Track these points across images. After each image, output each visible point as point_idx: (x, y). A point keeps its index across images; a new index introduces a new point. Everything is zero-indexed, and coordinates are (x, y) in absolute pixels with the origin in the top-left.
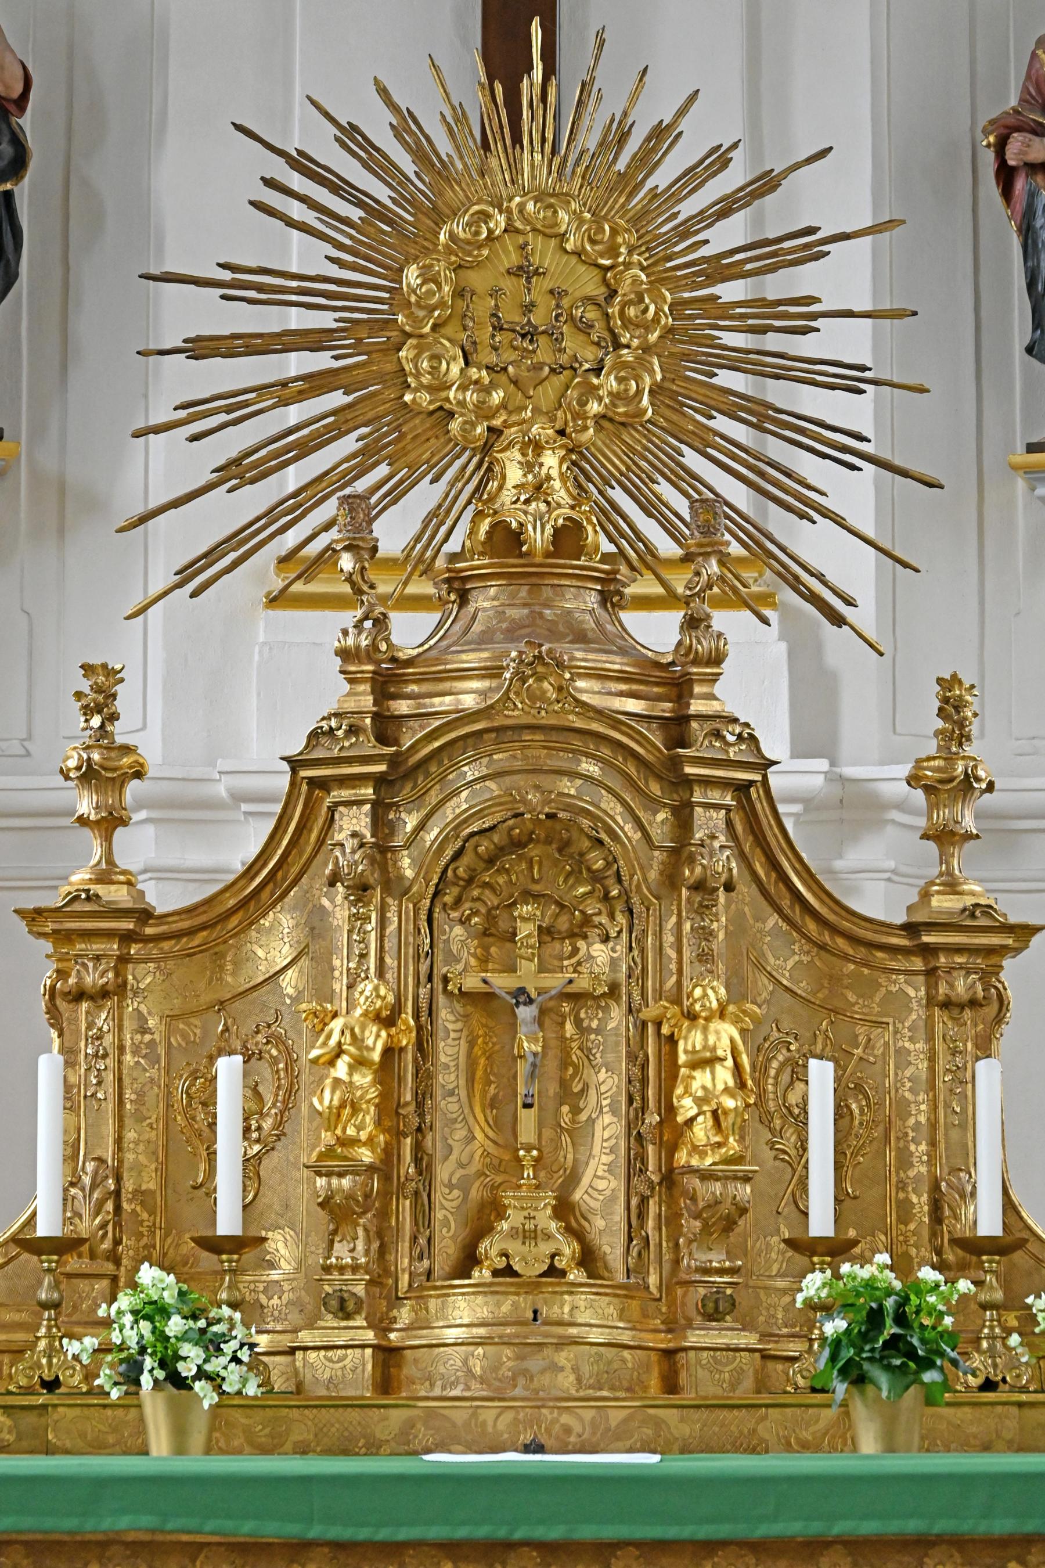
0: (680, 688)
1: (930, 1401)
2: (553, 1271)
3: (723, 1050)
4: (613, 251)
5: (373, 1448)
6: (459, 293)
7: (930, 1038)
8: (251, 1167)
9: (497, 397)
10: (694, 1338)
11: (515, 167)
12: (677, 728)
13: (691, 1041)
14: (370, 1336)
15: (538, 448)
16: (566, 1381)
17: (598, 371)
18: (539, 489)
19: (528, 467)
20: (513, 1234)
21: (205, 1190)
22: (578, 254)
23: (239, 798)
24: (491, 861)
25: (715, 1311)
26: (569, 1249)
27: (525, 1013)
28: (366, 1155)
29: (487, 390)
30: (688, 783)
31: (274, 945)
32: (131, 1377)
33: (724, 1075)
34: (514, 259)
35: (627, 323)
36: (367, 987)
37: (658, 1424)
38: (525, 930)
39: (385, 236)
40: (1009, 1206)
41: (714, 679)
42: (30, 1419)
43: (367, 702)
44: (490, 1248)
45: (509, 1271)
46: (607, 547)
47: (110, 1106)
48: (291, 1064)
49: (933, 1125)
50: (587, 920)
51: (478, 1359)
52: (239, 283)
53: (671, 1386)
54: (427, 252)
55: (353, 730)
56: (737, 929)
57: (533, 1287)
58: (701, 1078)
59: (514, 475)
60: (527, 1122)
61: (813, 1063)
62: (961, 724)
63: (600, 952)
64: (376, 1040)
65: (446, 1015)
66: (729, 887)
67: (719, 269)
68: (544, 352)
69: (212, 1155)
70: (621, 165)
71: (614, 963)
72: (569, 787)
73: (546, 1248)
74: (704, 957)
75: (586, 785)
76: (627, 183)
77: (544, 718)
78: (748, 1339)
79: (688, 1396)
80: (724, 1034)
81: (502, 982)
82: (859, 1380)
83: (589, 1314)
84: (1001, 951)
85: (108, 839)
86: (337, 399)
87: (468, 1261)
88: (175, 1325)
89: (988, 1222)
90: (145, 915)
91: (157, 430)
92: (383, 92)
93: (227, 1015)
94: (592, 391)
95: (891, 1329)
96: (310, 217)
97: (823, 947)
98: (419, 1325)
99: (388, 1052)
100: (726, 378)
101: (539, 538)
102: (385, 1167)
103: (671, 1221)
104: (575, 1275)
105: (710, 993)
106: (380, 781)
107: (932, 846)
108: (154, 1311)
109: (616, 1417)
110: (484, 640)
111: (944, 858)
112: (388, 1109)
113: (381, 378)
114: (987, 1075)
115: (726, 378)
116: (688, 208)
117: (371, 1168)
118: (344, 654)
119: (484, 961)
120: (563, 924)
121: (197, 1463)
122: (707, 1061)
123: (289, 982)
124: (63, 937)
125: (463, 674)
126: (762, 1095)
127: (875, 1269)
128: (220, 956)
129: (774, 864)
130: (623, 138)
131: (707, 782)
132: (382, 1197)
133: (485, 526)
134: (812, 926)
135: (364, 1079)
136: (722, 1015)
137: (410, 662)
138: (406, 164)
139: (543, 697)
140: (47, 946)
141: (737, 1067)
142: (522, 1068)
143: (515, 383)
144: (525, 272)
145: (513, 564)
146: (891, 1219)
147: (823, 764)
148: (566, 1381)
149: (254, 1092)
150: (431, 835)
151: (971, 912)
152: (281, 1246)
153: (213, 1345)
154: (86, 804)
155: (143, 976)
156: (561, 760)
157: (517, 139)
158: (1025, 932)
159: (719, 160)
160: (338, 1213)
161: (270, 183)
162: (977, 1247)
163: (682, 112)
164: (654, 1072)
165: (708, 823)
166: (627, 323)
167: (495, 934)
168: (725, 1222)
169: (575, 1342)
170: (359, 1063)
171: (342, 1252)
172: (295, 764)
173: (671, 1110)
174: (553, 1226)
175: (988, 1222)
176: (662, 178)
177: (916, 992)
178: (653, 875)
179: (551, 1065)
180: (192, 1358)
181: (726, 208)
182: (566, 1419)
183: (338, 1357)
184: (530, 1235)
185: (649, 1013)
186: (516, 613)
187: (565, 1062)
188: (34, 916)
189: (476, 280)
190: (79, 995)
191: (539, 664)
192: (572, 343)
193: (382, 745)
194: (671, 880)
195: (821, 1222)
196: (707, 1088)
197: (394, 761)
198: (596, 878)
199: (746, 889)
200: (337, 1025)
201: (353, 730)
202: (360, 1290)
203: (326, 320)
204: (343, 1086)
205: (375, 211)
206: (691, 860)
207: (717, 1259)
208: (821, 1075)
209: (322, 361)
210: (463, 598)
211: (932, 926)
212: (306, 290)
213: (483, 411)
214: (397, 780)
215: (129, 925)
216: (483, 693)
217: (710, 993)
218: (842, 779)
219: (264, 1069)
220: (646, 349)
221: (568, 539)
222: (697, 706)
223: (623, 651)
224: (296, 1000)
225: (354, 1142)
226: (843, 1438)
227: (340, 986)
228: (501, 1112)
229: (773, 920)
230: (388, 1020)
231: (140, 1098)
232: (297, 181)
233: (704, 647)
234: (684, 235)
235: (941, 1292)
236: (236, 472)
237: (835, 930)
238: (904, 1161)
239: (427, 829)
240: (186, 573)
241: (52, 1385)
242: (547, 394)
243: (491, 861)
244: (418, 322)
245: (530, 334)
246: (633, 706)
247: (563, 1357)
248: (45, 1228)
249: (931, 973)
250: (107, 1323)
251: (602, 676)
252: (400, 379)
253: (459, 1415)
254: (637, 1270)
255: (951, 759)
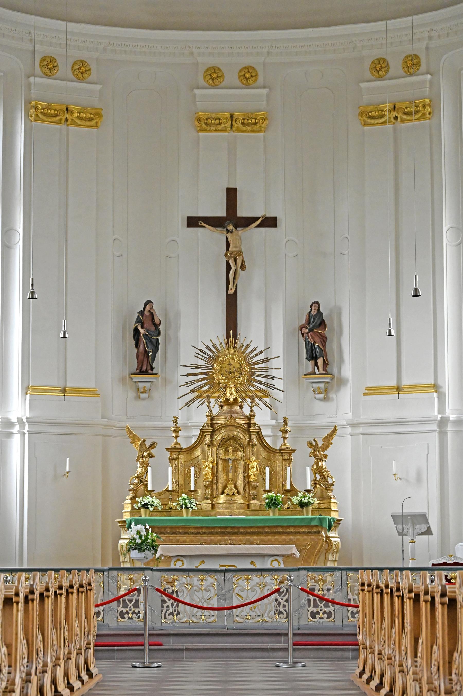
0: (250, 419)
1: (279, 510)
2: (234, 494)
3: (255, 466)
4: (241, 362)
5: (211, 516)
6: (222, 367)
7: (282, 464)
8: (196, 481)
9: (226, 381)
10: (251, 502)
11: (228, 350)
12: (249, 425)
13: (251, 465)
14: (210, 502)
15: (231, 388)
16: (235, 508)
17: (239, 377)
18: (231, 394)
19: (230, 390)
20: (229, 489)
21: (190, 484)
22: (237, 362)
23: (192, 426)
24: (225, 442)
25: (254, 499)
26: (236, 491)
27: (230, 461)
28: (210, 480)
29: (225, 380)
30: (251, 432)
31: (198, 452)
32: (181, 507)
33: (255, 469)
34: (228, 363)
35: (243, 371)
36: (210, 458)
37: (246, 513)
38: (230, 451)
39: (212, 360)
40: (291, 485)
41: (254, 418)
42: (169, 513)
43: (210, 422)
44: (226, 491)
45: (228, 494)
46: (240, 400)
47: (177, 474)
48: (200, 468)
49: (283, 475)
50: (238, 449)
51: (224, 505)
52: (193, 366)
53: (248, 508)
54: (217, 362)
55: (208, 426)
56: (257, 450)
57: (231, 496)
58: (252, 470)
59: (229, 391)
60: (230, 475)
61: (266, 468)
62: (286, 423)
63: (240, 453)
64: (211, 465)
65: (220, 462)
66: (256, 445)
67: (255, 363)
68: (232, 375)
69: (190, 479)
70: (242, 350)
71: (241, 455)
72: (235, 433)
73: (233, 491)
74: (253, 454)
75: (238, 433)
76: (243, 352)
77: (232, 424)
78: (258, 502)
79: (250, 509)
80: (255, 464)
81: (227, 457)
82: (270, 508)
83: (238, 499)
84: (291, 453)
85: (176, 439)
86: (206, 381)
87: (223, 493)
88: (187, 501)
89: (288, 487)
90: (182, 449)
91: (182, 386)
92: (211, 341)
93: (193, 462)
94: (238, 380)
95: (274, 501)
96: (202, 357)
97: (269, 452)
98: (217, 501)
99: (213, 466)
100: (256, 378)
101: (232, 400)
102: (213, 480)
103: (249, 488)
104: (237, 494)
105: (253, 458)
106: (211, 432)
107: (283, 439)
108: (184, 499)
109: (241, 512)
110: (225, 413)
111: (284, 441)
112: (213, 474)
113: (211, 379)
114: (288, 469)
115: (256, 378)
116: (251, 355)
117: (210, 481)
118: (207, 416)
119: (225, 454)
120: (235, 449)
121: (190, 517)
122: (253, 467)
123: (200, 457)
124: (170, 452)
125: (222, 418)
126: (260, 472)
127: (273, 494)
128: (191, 454)
129: (262, 442)
130: (242, 346)
131: (253, 432)
132: (213, 484)
133: (225, 398)
134: (267, 449)
135: (210, 470)
136: (255, 461)
137: (215, 416)
138: (214, 350)
139: (232, 422)
140: (169, 453)
141: (257, 468)
142: (230, 468)
143: (229, 379)
144: (230, 364)
145: (228, 404)
146: (277, 487)
147: (275, 421)
148: (235, 508)
149: (196, 471)
150: (218, 439)
151: (287, 448)
152: (199, 491)
153: (192, 503)
154: (174, 434)
155: (181, 456)
156: (235, 429)
157: (229, 347)
158: (294, 451)
159: (255, 349)
160: (206, 487)
161: (196, 353)
162: (287, 491)
163: (250, 343)
164: (247, 468)
165: (254, 437)
166: (243, 371)
167: (226, 451)
168: (255, 488)
169: (236, 503)
170: (209, 468)
171: (207, 492)
172: (201, 430)
173: (248, 474)
174: (234, 488)
175: (288, 487)
176: (248, 351)
177: (280, 458)
178: (246, 443)
179: (234, 467)
180: (189, 505)
181: (256, 355)
182: (235, 512)
183: (207, 505)
184: (230, 489)
185: (246, 461)
186: (229, 410)
187: (235, 467)
188: (167, 449)
189: (224, 366)
190: (173, 459)
191: (231, 418)
192: (236, 374)
193: (212, 426)
194: (249, 444)
195: (267, 488)
196: (253, 471)
197: (213, 430)
198: (239, 444)
199: (259, 445)
200: (206, 463)
201: (208, 426)
202: (209, 497)
203: (204, 371)
204: (207, 471)
205: (210, 357)
206: (251, 442)
207: (254, 492)
208: (267, 469)
209: (204, 376)
210: (222, 408)
211: (282, 450)
212: (201, 367)
213: (224, 383)
214: (213, 433)
215: (179, 450)
216: (225, 421)
217: (253, 458)
218: (278, 422)
219: (197, 468)
220: (246, 374)
221: (235, 400)
222: (252, 422)
223: (242, 415)
224: (201, 460)
225: (208, 478)
226: (269, 515)
227: (206, 458)
228: (227, 473)
229: (262, 449)
230: (213, 462)
231: (181, 472)
232: (199, 352)
233: (253, 414)
234: (251, 359)
235: (281, 496)
236: (192, 391)
237: (270, 450)
238: (279, 479)
239: (218, 438)
240: (186, 404)
241: (171, 509)
242: (233, 380)
243: (225, 442)
244: (216, 371)
245: (230, 373)
246: (244, 422)
247: (235, 505)
248: (170, 489)
249: (282, 456)
250: (178, 501)
251: (239, 419)
252: (214, 379)
253: (222, 512)
254: (244, 494)
255: (285, 428)
